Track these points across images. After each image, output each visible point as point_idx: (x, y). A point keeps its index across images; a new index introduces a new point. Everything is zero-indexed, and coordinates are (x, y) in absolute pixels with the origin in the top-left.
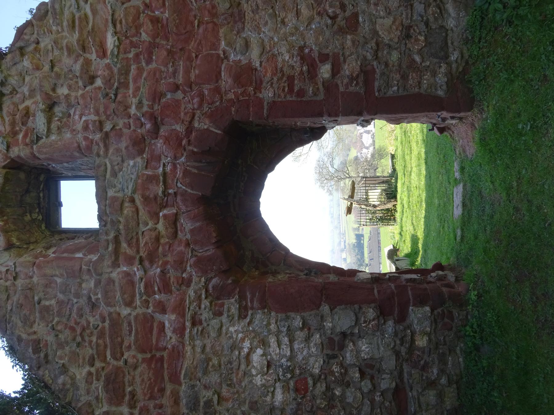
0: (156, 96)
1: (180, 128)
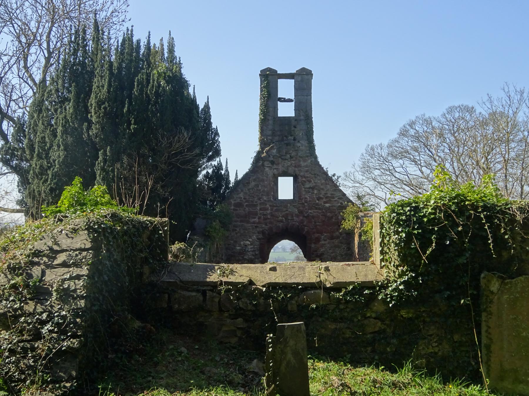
0: (313, 217)
1: (305, 223)
